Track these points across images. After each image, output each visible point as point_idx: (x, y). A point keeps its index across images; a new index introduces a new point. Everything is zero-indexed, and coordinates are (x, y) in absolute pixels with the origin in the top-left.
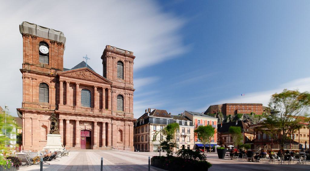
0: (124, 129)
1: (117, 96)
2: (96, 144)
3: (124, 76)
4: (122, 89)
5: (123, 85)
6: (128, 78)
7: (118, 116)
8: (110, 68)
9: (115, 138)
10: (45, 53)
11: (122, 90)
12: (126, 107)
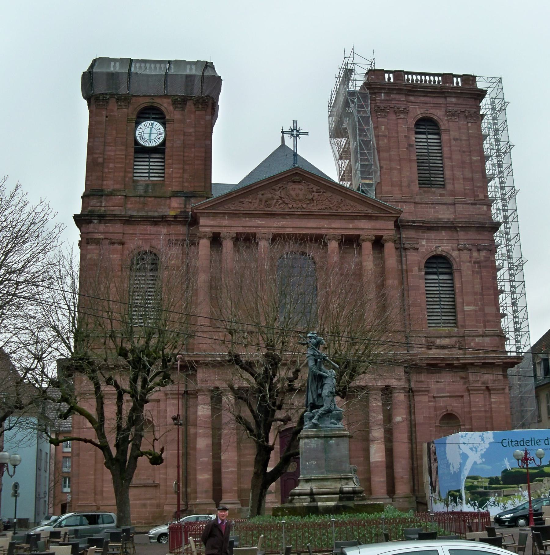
1: (423, 265)
4: (444, 228)
10: (153, 144)
11: (444, 233)
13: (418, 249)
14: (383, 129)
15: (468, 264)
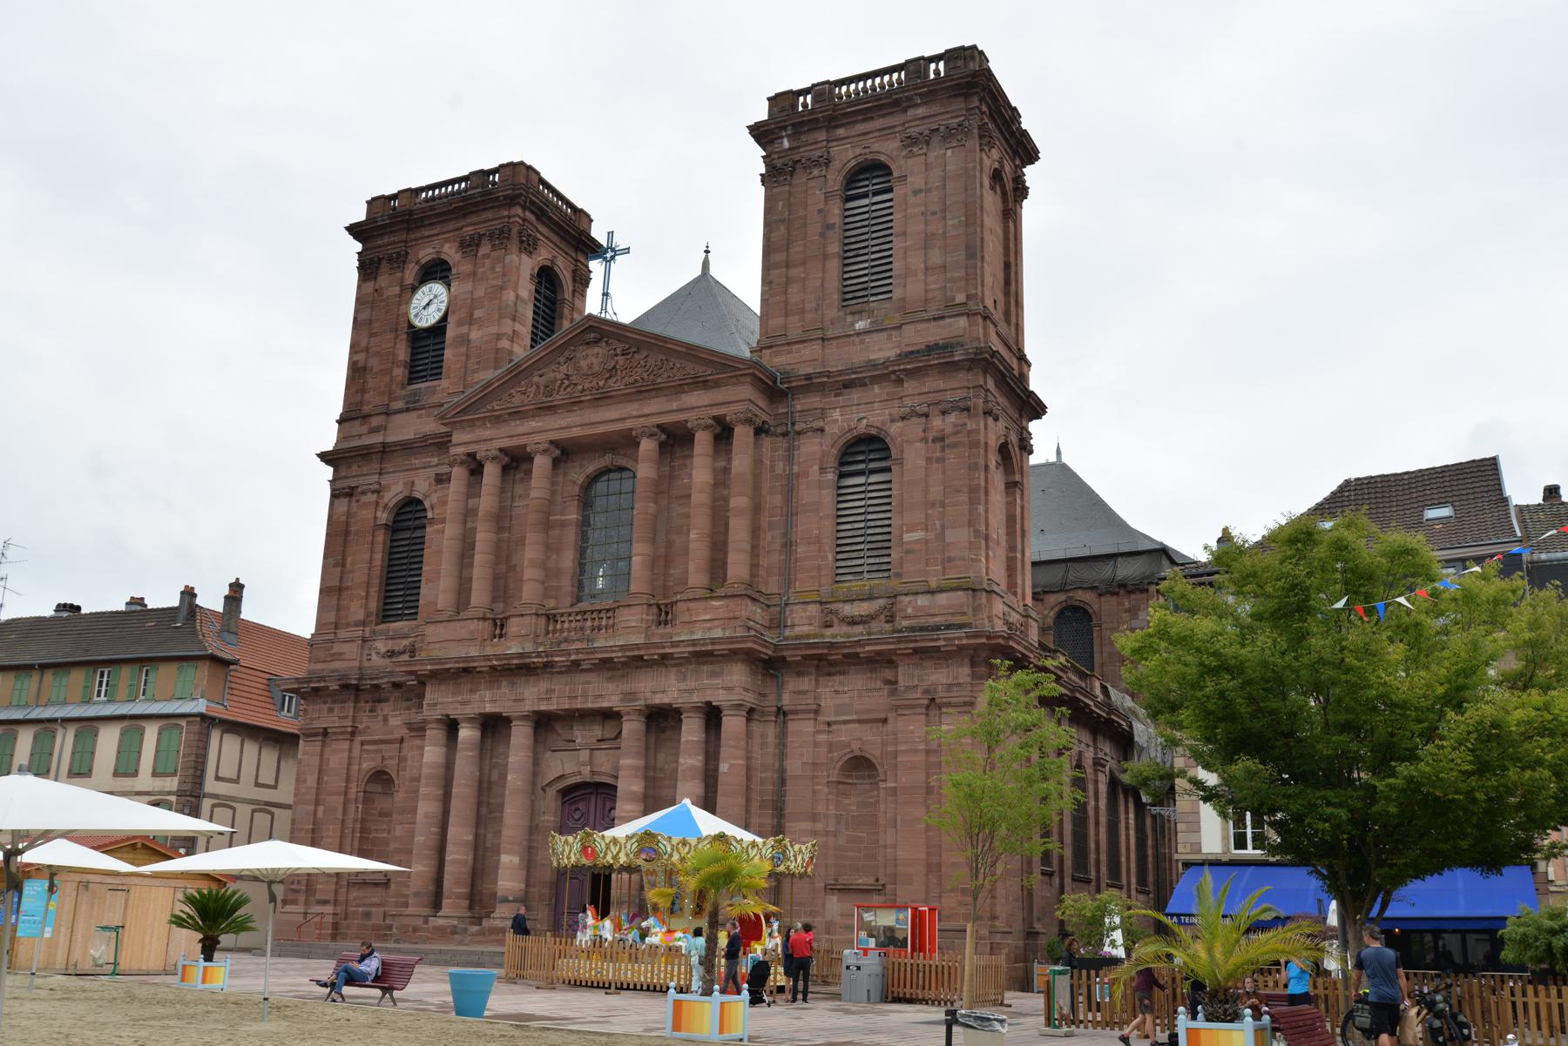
4: (875, 379)
5: (883, 350)
7: (837, 633)
11: (876, 389)
13: (822, 430)
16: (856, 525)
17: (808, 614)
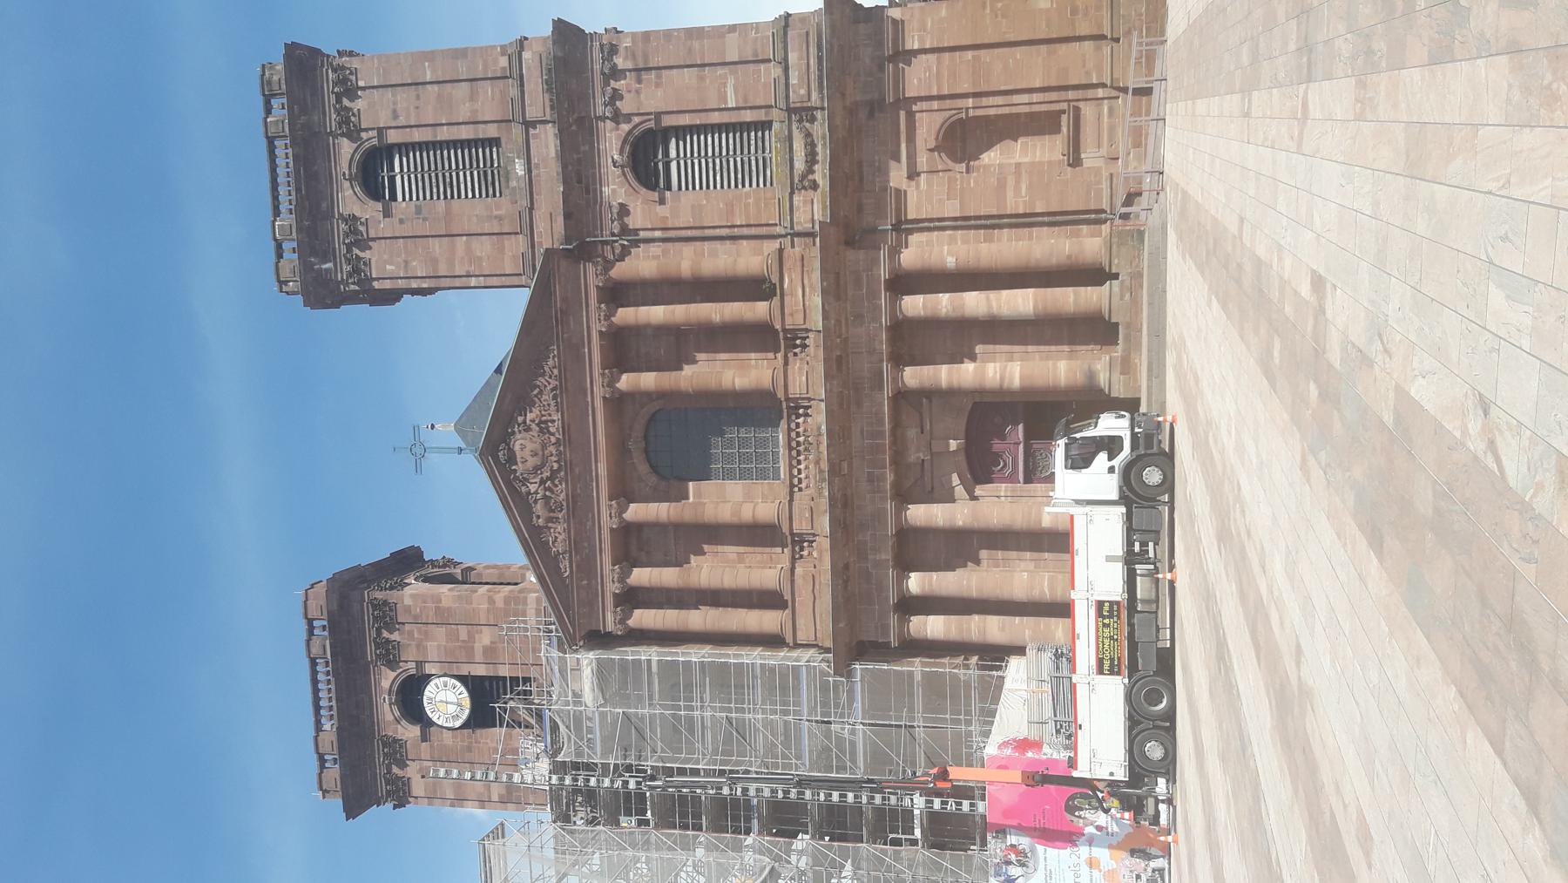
0: (935, 105)
2: (1091, 375)
3: (465, 133)
5: (547, 142)
6: (473, 97)
7: (821, 175)
8: (435, 261)
9: (1030, 187)
12: (724, 99)
14: (393, 268)
15: (642, 96)
16: (718, 168)
17: (801, 204)
